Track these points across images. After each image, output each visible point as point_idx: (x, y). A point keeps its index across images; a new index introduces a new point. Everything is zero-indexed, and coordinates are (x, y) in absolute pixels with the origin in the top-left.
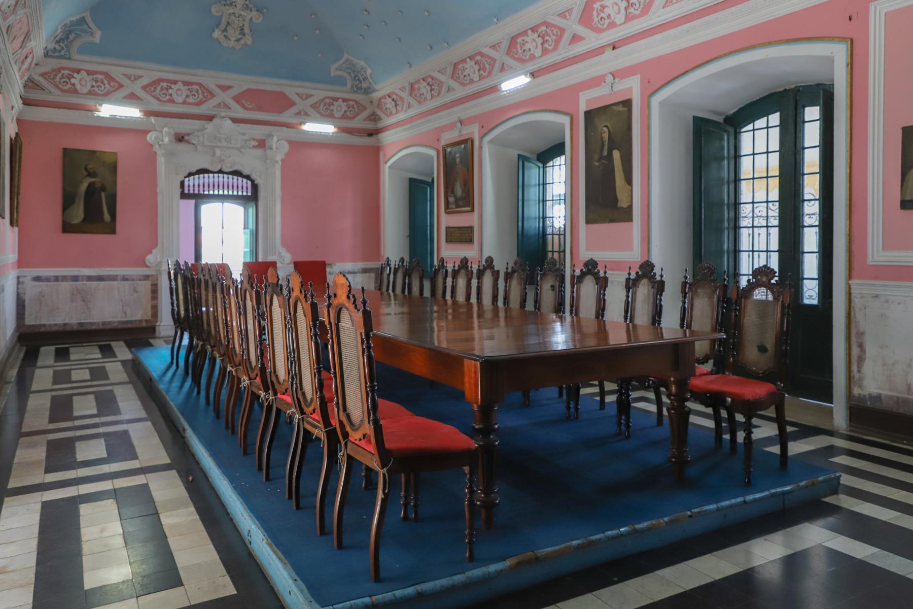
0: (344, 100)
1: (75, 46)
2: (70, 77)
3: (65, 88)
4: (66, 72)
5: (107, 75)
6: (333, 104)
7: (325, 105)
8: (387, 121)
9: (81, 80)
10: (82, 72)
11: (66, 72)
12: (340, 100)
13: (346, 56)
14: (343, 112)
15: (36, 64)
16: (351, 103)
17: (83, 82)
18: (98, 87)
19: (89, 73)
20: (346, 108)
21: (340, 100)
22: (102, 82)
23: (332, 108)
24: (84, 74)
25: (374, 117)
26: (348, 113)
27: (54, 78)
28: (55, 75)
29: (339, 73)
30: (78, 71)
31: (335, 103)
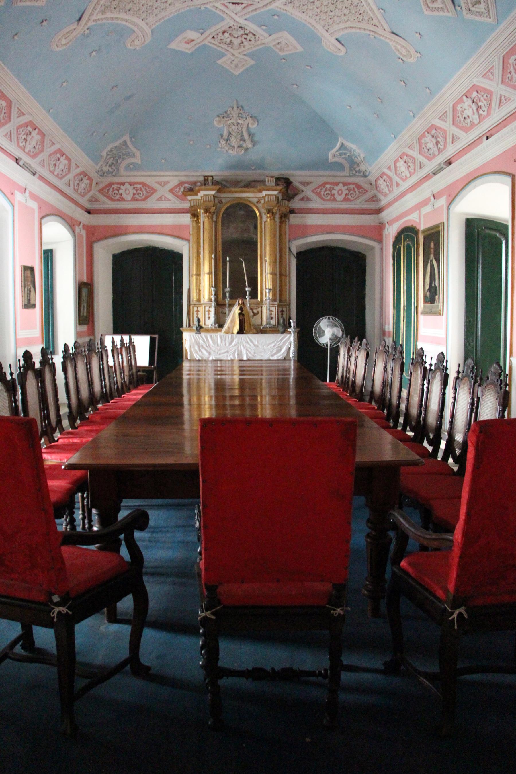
0: (344, 184)
1: (123, 165)
2: (118, 189)
3: (116, 198)
4: (115, 186)
5: (143, 184)
6: (333, 189)
7: (326, 190)
8: (384, 201)
9: (126, 190)
10: (126, 184)
11: (115, 186)
12: (341, 185)
13: (340, 140)
14: (343, 195)
15: (97, 183)
16: (352, 186)
17: (127, 192)
18: (138, 194)
19: (131, 184)
20: (347, 192)
21: (341, 185)
22: (141, 190)
23: (333, 192)
24: (127, 185)
25: (374, 199)
26: (349, 196)
27: (108, 192)
28: (109, 190)
29: (336, 159)
30: (123, 184)
31: (335, 187)
